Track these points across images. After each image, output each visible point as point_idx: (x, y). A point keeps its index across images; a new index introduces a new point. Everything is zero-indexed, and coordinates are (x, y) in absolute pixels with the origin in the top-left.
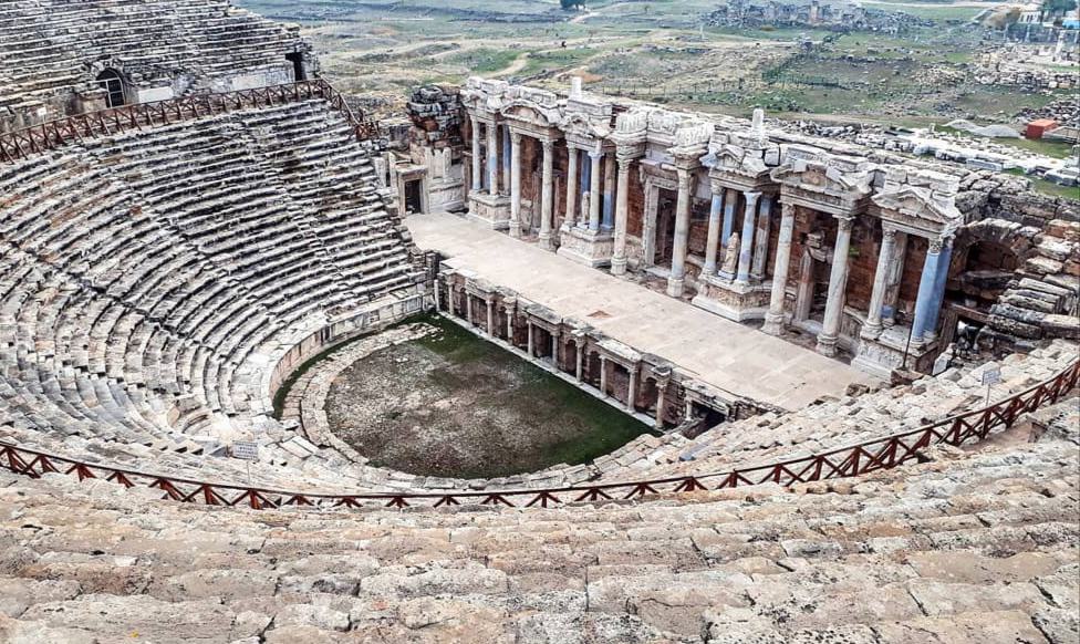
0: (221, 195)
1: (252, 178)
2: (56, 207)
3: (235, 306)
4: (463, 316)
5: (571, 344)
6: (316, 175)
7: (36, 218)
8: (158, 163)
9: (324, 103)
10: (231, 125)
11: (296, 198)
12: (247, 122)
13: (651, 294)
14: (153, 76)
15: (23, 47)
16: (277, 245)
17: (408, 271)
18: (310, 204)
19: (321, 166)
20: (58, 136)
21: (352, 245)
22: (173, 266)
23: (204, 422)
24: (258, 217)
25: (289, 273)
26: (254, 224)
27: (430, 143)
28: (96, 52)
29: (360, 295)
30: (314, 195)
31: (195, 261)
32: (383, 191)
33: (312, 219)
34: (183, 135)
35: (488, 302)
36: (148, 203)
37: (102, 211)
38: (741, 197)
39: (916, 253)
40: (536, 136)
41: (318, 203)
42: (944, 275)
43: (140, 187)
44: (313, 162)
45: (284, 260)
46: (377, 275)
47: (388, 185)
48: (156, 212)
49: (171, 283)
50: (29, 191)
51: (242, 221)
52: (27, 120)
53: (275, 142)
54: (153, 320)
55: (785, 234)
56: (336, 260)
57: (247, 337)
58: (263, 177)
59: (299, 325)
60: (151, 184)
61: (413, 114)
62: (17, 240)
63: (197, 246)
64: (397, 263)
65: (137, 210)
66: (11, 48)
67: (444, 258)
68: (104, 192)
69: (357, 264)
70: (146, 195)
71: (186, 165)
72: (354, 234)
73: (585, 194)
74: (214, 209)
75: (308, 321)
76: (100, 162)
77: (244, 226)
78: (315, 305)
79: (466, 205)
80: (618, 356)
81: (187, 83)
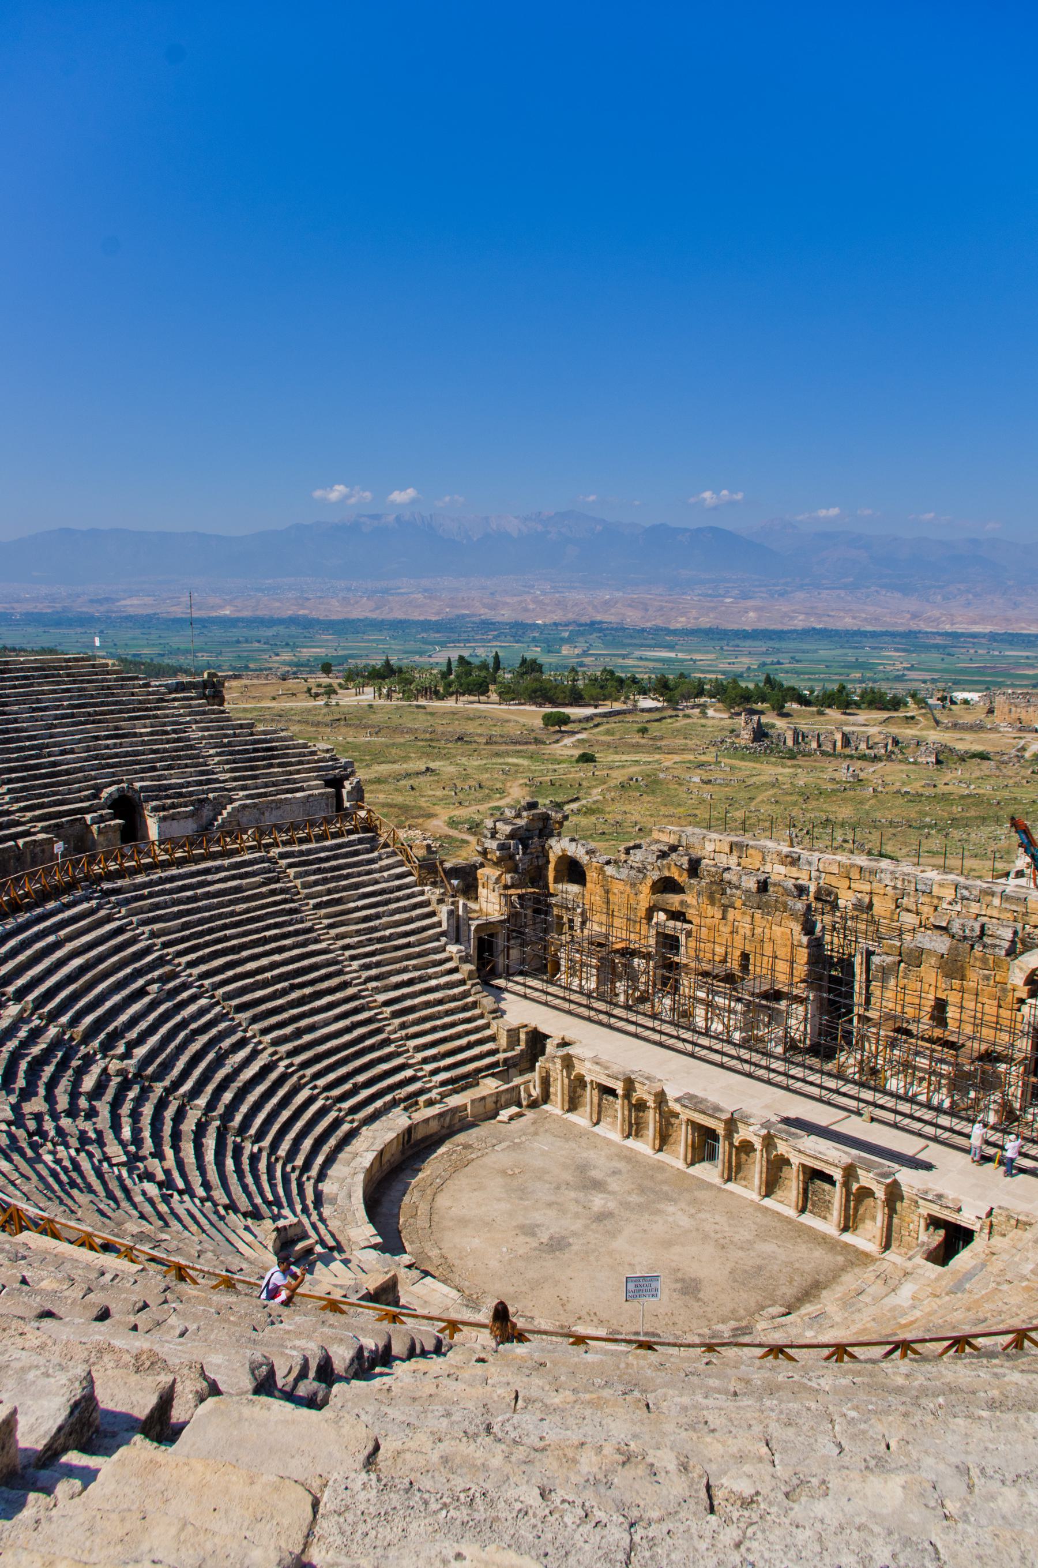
1: (297, 933)
9: (373, 840)
26: (307, 991)
29: (443, 1084)
35: (620, 1092)
45: (347, 1038)
58: (310, 930)
78: (388, 1098)
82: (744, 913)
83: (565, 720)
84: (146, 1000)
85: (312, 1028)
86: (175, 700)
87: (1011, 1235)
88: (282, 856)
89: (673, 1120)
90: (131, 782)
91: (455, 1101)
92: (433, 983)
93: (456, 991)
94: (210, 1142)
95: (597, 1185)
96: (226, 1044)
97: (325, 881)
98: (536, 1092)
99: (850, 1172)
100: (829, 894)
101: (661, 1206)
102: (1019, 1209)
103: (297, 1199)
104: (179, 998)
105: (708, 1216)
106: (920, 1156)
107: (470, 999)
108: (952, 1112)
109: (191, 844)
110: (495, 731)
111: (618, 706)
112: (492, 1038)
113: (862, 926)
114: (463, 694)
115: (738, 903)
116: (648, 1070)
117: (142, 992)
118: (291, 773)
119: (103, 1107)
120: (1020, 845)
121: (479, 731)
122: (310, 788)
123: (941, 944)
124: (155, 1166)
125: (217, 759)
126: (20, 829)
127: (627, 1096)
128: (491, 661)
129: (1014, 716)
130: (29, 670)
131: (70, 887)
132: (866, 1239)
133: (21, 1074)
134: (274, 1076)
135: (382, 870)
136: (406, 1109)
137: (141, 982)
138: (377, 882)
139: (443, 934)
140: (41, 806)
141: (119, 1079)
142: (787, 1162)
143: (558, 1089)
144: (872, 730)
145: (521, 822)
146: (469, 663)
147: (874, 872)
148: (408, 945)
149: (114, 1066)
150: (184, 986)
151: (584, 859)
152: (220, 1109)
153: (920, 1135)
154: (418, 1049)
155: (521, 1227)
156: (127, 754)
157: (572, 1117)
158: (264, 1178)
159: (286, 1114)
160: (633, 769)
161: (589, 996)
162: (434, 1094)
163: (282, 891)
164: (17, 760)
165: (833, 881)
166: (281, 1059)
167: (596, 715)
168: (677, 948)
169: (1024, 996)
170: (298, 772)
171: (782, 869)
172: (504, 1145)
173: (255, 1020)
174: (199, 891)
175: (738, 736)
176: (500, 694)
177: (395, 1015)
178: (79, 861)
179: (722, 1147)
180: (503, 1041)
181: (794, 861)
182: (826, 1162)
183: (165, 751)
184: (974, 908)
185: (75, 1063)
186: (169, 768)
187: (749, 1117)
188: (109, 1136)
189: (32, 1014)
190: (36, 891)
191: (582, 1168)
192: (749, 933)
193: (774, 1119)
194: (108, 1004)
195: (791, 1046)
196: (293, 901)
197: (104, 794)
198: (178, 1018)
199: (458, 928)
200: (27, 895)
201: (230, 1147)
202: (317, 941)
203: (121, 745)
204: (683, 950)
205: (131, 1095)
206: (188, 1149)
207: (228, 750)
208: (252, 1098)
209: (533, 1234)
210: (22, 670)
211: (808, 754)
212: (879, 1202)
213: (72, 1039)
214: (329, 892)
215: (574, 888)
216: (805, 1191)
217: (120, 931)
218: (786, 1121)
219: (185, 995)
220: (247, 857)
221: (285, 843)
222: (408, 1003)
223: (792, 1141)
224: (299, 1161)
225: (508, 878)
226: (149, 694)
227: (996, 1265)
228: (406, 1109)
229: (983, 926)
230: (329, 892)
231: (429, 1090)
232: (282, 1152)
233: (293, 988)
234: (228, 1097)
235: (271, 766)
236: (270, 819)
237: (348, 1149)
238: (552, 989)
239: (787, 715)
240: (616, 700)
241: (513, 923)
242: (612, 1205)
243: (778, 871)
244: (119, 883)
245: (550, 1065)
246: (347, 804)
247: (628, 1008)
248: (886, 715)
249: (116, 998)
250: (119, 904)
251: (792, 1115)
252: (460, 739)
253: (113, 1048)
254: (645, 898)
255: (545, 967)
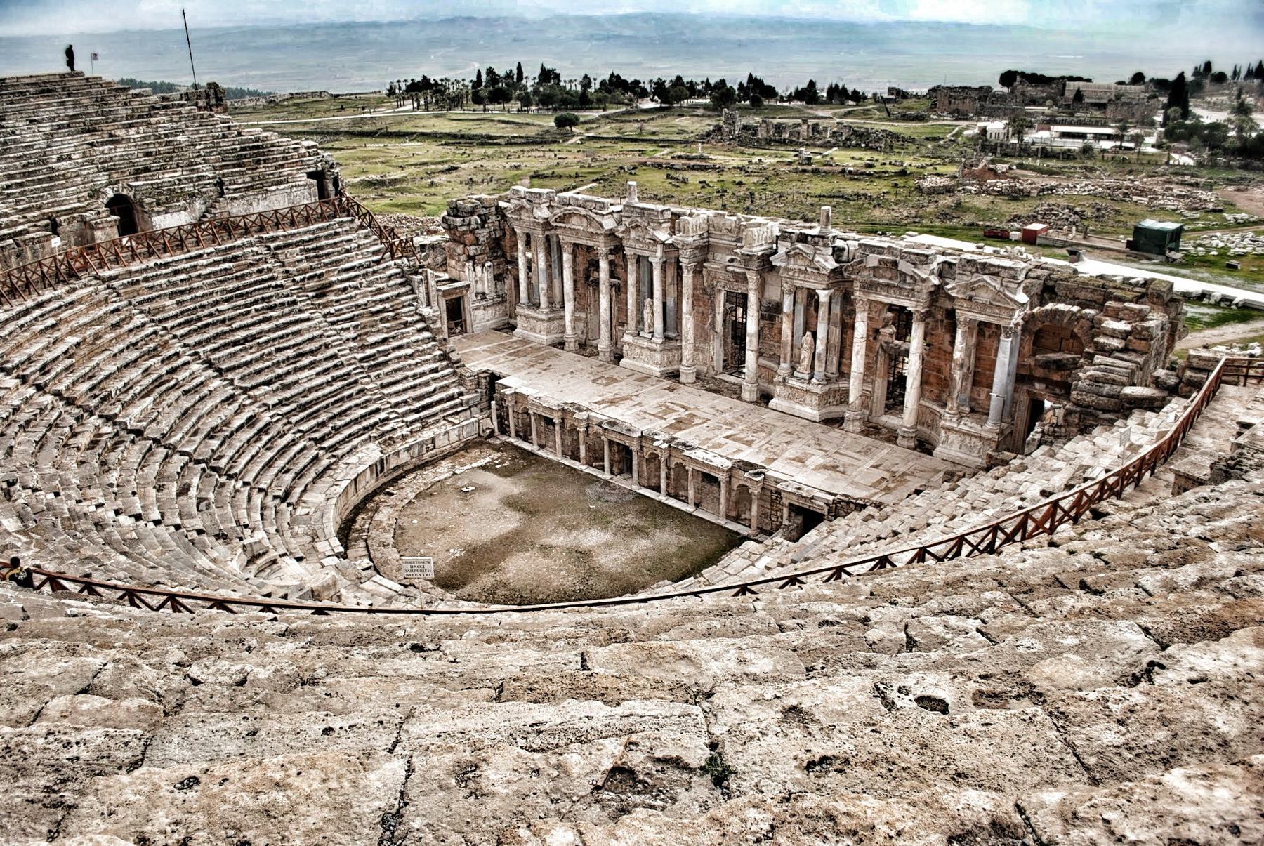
0: (252, 325)
1: (282, 304)
2: (78, 344)
3: (282, 442)
4: (526, 439)
5: (653, 458)
6: (351, 298)
7: (57, 358)
8: (182, 292)
9: (352, 221)
10: (255, 249)
11: (334, 323)
12: (272, 245)
13: (723, 402)
14: (168, 201)
15: (24, 175)
16: (318, 374)
17: (461, 394)
18: (348, 329)
19: (356, 288)
20: (70, 267)
21: (396, 371)
22: (210, 404)
23: (275, 566)
24: (294, 346)
25: (334, 403)
26: (290, 353)
27: (471, 258)
28: (103, 178)
29: (413, 422)
30: (351, 319)
31: (232, 396)
32: (426, 311)
33: (352, 344)
34: (205, 262)
35: (556, 421)
36: (175, 337)
37: (128, 347)
38: (812, 296)
39: (987, 341)
40: (590, 243)
41: (356, 326)
42: (1015, 361)
43: (166, 320)
44: (347, 284)
45: (328, 390)
46: (428, 401)
47: (429, 304)
48: (185, 345)
49: (214, 421)
50: (46, 328)
51: (279, 350)
52: (34, 253)
53: (305, 265)
54: (198, 462)
55: (861, 329)
56: (383, 386)
57: (300, 475)
59: (352, 459)
60: (176, 316)
61: (451, 229)
62: (41, 381)
63: (232, 380)
64: (447, 387)
65: (165, 345)
66: (10, 177)
67: (500, 378)
68: (126, 328)
69: (405, 390)
70: (172, 328)
71: (211, 294)
72: (399, 358)
73: (648, 301)
74: (246, 340)
75: (360, 455)
76: (119, 295)
77: (281, 356)
79: (512, 321)
80: (707, 465)
81: (203, 207)
128: (515, 71)
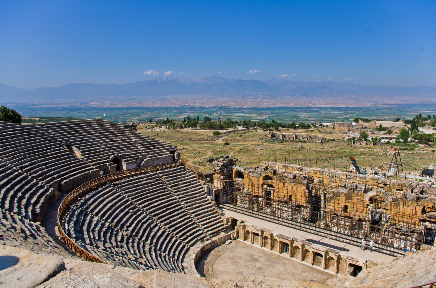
1: (167, 194)
9: (184, 168)
17: (222, 225)
26: (172, 210)
29: (210, 234)
35: (260, 234)
45: (183, 223)
78: (196, 239)
82: (290, 184)
83: (219, 134)
84: (130, 214)
85: (174, 221)
86: (127, 130)
87: (373, 267)
88: (161, 173)
89: (275, 241)
90: (117, 154)
91: (214, 239)
92: (205, 207)
93: (211, 209)
94: (153, 253)
95: (256, 260)
96: (152, 226)
97: (173, 180)
98: (235, 236)
99: (327, 253)
100: (311, 178)
101: (275, 265)
102: (374, 260)
103: (178, 268)
104: (138, 214)
105: (288, 267)
106: (345, 248)
107: (215, 211)
108: (351, 236)
109: (136, 171)
110: (200, 137)
111: (233, 129)
112: (222, 221)
113: (321, 187)
114: (190, 127)
115: (288, 182)
116: (267, 228)
117: (128, 213)
118: (160, 150)
119: (124, 244)
120: (352, 164)
121: (195, 137)
122: (166, 154)
123: (345, 191)
124: (143, 261)
125: (140, 147)
126: (90, 168)
127: (262, 235)
129: (340, 129)
130: (86, 123)
131: (105, 184)
132: (331, 270)
133: (102, 236)
134: (166, 234)
135: (187, 176)
136: (201, 242)
137: (127, 210)
138: (186, 180)
139: (206, 193)
140: (94, 161)
141: (127, 237)
142: (308, 251)
143: (241, 234)
144: (303, 134)
145: (225, 162)
146: (190, 119)
147: (323, 172)
148: (197, 197)
149: (125, 233)
150: (139, 210)
151: (243, 171)
152: (154, 244)
153: (344, 242)
154: (203, 225)
155: (238, 272)
156: (116, 146)
157: (245, 242)
158: (168, 262)
159: (170, 245)
160: (241, 147)
161: (246, 209)
162: (208, 237)
163: (161, 183)
164: (86, 148)
165: (312, 175)
166: (167, 229)
167: (227, 132)
168: (271, 194)
169: (368, 203)
170: (162, 150)
171: (298, 172)
172: (229, 250)
173: (158, 219)
174: (139, 184)
175: (267, 137)
176: (200, 127)
177: (196, 216)
178: (106, 176)
179: (290, 248)
180: (225, 222)
181: (301, 170)
182: (320, 250)
183: (126, 145)
184: (352, 181)
185: (115, 233)
186: (128, 149)
187: (297, 239)
188: (128, 253)
189: (101, 220)
190: (96, 185)
191: (251, 256)
192: (291, 190)
193: (304, 240)
194: (120, 216)
195: (305, 220)
196: (165, 185)
197: (111, 157)
198: (138, 219)
199: (209, 191)
200: (94, 186)
201: (158, 254)
202: (172, 196)
203: (114, 144)
204: (272, 195)
205: (131, 241)
206: (148, 255)
207: (143, 144)
208: (161, 240)
209: (242, 274)
210: (84, 123)
211: (286, 141)
212: (335, 261)
213: (112, 226)
214: (174, 183)
215: (241, 179)
216: (314, 259)
217: (120, 195)
218: (307, 240)
219: (139, 213)
220: (151, 174)
221: (161, 170)
222: (199, 213)
223: (310, 246)
224: (176, 258)
225: (222, 177)
226: (120, 129)
227: (371, 276)
228: (201, 242)
229: (356, 185)
230: (174, 183)
231: (207, 236)
232: (171, 255)
233: (168, 209)
234: (155, 240)
235: (155, 148)
236: (156, 163)
237: (188, 253)
238: (236, 207)
239: (279, 131)
240: (232, 128)
241: (224, 190)
242: (261, 265)
243: (297, 173)
244: (118, 182)
245: (239, 228)
246: (176, 158)
247: (258, 211)
248: (306, 130)
249: (122, 214)
250: (119, 188)
251: (309, 238)
252: (191, 140)
253: (123, 228)
254: (261, 181)
255: (233, 201)
